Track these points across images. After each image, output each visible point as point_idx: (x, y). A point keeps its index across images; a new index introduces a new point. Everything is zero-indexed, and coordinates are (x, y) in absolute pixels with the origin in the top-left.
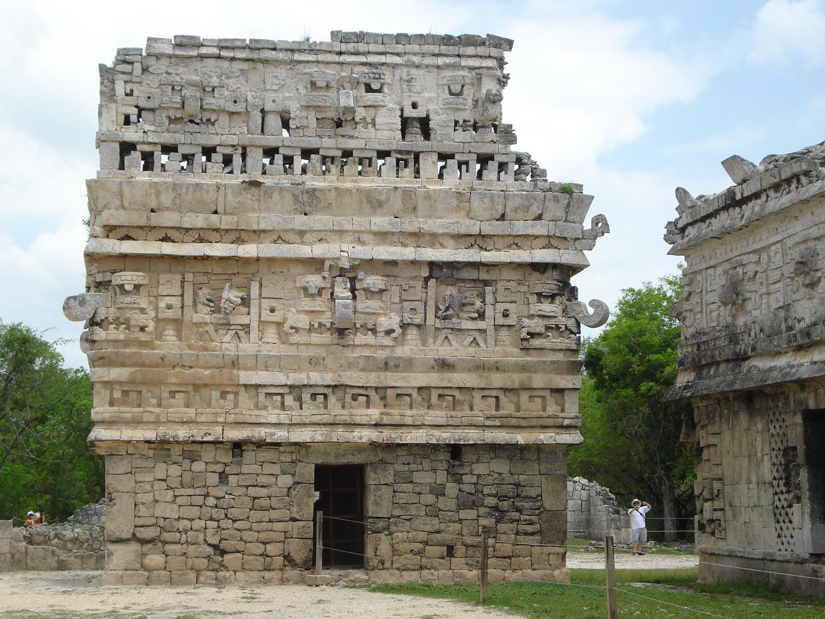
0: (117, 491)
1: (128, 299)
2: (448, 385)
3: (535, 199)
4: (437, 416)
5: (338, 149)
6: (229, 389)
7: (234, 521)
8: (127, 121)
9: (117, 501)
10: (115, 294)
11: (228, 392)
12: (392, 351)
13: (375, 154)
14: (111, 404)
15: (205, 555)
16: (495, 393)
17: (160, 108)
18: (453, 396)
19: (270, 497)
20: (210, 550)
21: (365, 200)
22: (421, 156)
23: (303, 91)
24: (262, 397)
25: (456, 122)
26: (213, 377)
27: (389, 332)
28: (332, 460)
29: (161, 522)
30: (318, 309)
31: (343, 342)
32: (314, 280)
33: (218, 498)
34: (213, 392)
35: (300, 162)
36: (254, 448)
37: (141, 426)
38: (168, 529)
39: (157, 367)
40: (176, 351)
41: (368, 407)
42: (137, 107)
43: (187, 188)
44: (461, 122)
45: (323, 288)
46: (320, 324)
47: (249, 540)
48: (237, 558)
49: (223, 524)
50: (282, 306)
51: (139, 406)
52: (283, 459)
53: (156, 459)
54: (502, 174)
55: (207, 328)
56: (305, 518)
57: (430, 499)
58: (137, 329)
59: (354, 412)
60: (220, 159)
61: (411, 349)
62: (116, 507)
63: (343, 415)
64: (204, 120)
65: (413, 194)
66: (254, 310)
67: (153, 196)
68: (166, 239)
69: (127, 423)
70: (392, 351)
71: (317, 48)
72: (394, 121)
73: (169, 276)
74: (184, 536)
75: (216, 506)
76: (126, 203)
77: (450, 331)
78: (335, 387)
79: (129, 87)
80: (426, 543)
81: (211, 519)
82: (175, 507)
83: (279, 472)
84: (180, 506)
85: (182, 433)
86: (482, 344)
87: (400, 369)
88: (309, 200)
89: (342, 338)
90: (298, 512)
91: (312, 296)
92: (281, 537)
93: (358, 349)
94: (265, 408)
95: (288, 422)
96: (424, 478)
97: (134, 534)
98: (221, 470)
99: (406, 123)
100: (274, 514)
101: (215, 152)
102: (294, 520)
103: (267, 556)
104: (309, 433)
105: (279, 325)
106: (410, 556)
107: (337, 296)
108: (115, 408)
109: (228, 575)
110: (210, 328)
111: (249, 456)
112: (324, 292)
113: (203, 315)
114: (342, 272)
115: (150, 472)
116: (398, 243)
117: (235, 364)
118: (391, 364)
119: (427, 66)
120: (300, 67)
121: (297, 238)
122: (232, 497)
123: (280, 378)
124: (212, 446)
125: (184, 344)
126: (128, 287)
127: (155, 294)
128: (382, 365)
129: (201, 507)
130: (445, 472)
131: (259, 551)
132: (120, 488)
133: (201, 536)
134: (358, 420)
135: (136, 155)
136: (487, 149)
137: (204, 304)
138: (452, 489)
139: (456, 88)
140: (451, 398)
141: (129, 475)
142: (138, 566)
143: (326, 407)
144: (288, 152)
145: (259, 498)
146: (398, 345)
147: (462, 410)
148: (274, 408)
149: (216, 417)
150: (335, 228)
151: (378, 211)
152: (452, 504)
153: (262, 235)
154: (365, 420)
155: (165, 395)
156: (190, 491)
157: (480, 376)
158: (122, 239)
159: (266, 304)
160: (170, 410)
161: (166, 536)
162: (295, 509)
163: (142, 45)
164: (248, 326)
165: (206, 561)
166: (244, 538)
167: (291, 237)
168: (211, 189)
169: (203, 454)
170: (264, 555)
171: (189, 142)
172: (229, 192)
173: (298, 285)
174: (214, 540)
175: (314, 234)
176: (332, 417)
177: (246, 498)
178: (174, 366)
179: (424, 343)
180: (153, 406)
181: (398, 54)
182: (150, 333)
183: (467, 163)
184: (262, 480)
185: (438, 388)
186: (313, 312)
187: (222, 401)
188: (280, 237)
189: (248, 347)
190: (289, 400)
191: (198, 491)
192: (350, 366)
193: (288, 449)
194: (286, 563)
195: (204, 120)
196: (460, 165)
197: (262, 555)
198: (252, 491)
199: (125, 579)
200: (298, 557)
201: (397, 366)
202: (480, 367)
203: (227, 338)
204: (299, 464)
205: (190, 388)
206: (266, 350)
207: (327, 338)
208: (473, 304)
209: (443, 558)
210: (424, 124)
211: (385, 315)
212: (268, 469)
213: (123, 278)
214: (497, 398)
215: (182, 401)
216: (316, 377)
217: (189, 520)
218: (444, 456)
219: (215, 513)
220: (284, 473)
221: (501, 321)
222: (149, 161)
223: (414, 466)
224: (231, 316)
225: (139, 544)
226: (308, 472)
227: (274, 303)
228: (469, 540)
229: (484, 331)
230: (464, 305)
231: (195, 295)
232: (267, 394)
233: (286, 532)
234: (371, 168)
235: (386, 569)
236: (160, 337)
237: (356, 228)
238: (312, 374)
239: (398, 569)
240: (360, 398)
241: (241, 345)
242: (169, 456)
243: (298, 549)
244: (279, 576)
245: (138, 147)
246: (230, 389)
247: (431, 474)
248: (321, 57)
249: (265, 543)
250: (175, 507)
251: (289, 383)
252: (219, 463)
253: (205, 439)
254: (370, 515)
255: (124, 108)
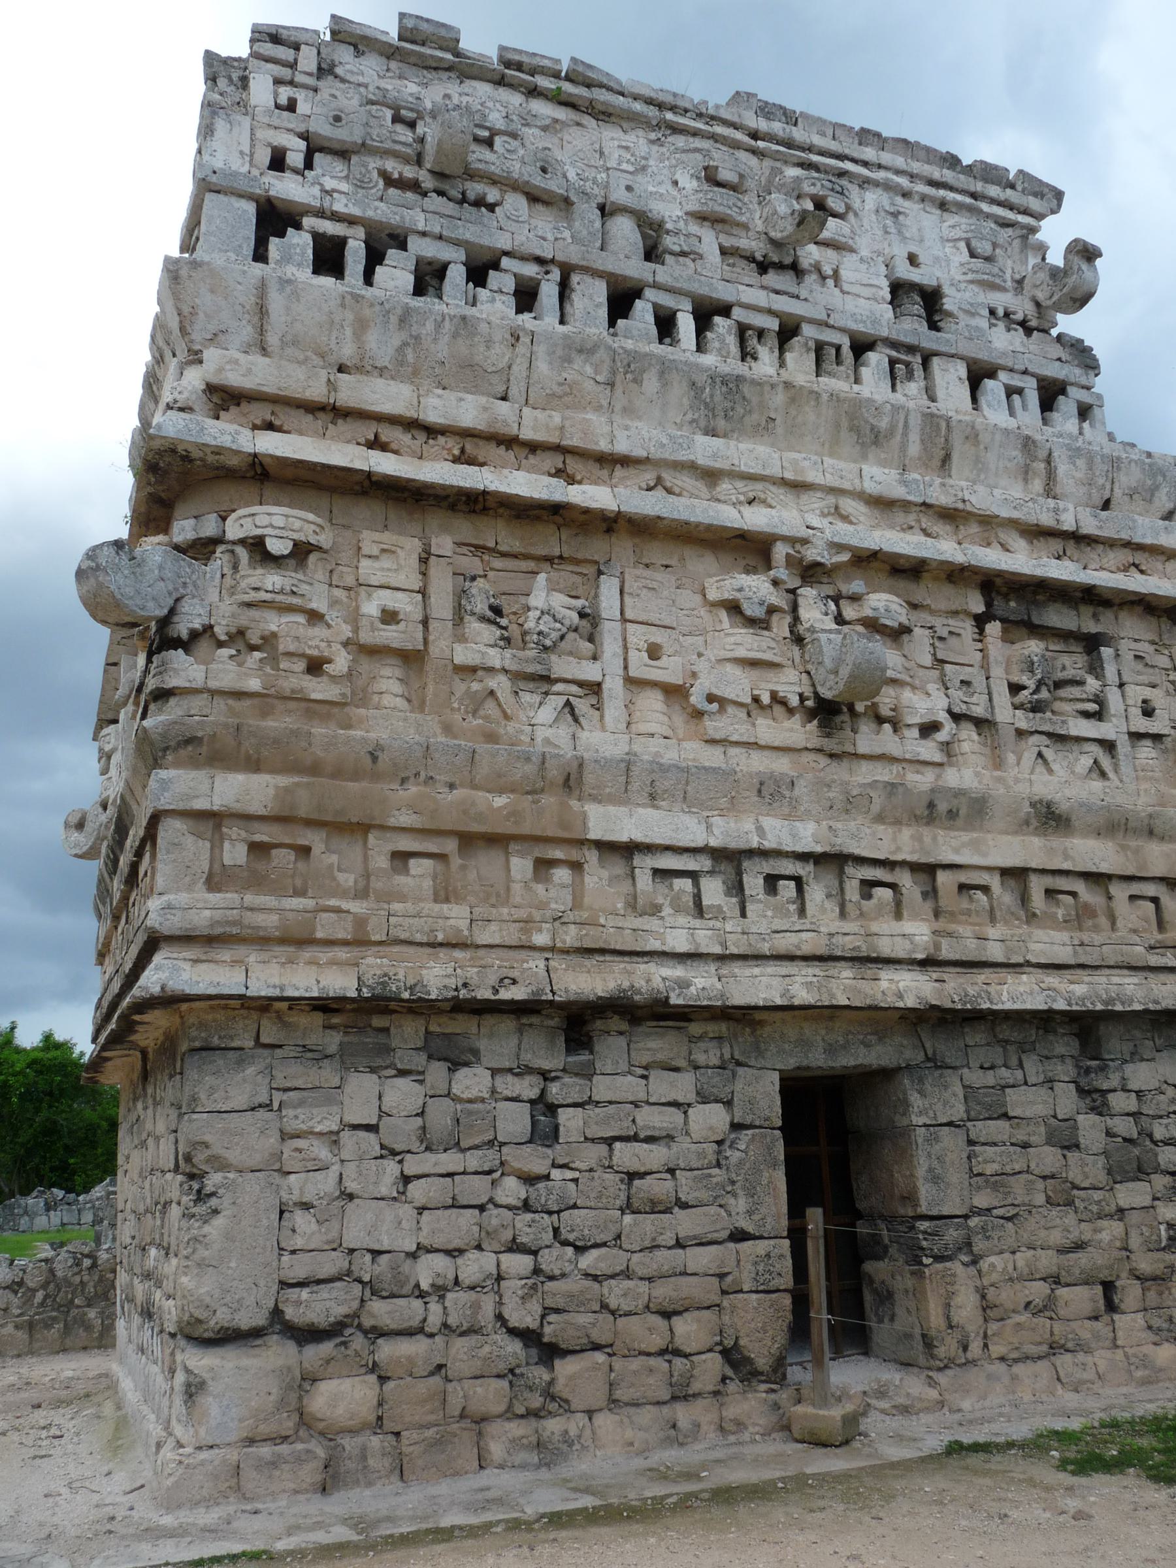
0: (222, 1165)
1: (273, 580)
2: (1066, 866)
3: (1164, 476)
4: (1050, 943)
5: (770, 312)
6: (558, 854)
7: (580, 1250)
8: (278, 162)
9: (223, 1202)
10: (235, 567)
11: (552, 863)
12: (939, 777)
13: (846, 342)
14: (213, 883)
15: (502, 1367)
16: (1150, 890)
17: (363, 148)
18: (1074, 894)
19: (671, 1171)
20: (515, 1347)
21: (845, 423)
22: (936, 362)
23: (688, 183)
24: (644, 880)
25: (992, 312)
26: (514, 814)
27: (928, 729)
28: (818, 1059)
29: (365, 1267)
30: (768, 656)
31: (831, 745)
32: (756, 588)
33: (530, 1180)
34: (515, 862)
35: (686, 324)
36: (624, 1026)
37: (307, 953)
38: (387, 1287)
39: (356, 776)
40: (412, 736)
41: (898, 916)
42: (305, 136)
43: (439, 325)
44: (1001, 312)
45: (772, 610)
46: (774, 695)
47: (625, 1308)
48: (596, 1367)
49: (551, 1259)
50: (677, 647)
51: (300, 893)
52: (701, 1058)
53: (346, 1060)
54: (1086, 425)
55: (492, 683)
56: (767, 1230)
57: (1048, 1158)
58: (301, 666)
59: (875, 927)
60: (510, 285)
61: (977, 774)
62: (219, 1221)
63: (849, 935)
64: (471, 196)
65: (943, 425)
66: (610, 646)
67: (348, 332)
68: (375, 444)
69: (262, 941)
70: (939, 777)
71: (711, 111)
72: (875, 282)
73: (388, 538)
74: (435, 1307)
75: (526, 1206)
76: (273, 340)
77: (1044, 740)
78: (818, 859)
79: (285, 93)
80: (1056, 1280)
81: (515, 1247)
82: (406, 1212)
83: (691, 1097)
84: (421, 1210)
85: (437, 977)
86: (1111, 775)
87: (959, 822)
88: (724, 405)
89: (828, 735)
90: (750, 1213)
91: (752, 622)
92: (706, 1290)
93: (865, 766)
94: (655, 910)
95: (717, 950)
96: (1028, 1102)
97: (277, 1312)
98: (533, 1093)
99: (899, 290)
100: (685, 1223)
101: (496, 266)
102: (739, 1236)
103: (678, 1353)
104: (775, 982)
105: (675, 693)
106: (1023, 1318)
107: (812, 630)
108: (229, 897)
109: (575, 1424)
110: (501, 684)
111: (611, 1049)
112: (775, 618)
113: (480, 645)
114: (811, 572)
115: (329, 1101)
116: (917, 530)
117: (571, 781)
118: (942, 807)
119: (923, 198)
120: (680, 141)
121: (701, 486)
122: (570, 1175)
123: (690, 829)
124: (508, 1024)
125: (432, 724)
126: (276, 546)
127: (350, 581)
128: (922, 811)
129: (482, 1208)
130: (1072, 1086)
131: (657, 1342)
132: (233, 1156)
133: (488, 1305)
134: (886, 948)
135: (300, 242)
136: (1055, 371)
137: (483, 619)
138: (1090, 1128)
139: (984, 247)
140: (1069, 899)
141: (262, 1114)
142: (288, 1424)
143: (802, 912)
144: (667, 300)
145: (642, 1175)
146: (951, 765)
147: (1096, 929)
148: (678, 910)
149: (527, 932)
150: (789, 475)
151: (872, 452)
152: (1096, 1171)
153: (619, 472)
154: (900, 949)
155: (381, 862)
156: (450, 1161)
157: (1124, 848)
158: (255, 427)
159: (638, 636)
160: (396, 907)
161: (381, 1312)
162: (740, 1204)
163: (321, 25)
164: (594, 689)
165: (504, 1384)
166: (613, 1304)
167: (685, 481)
168: (497, 337)
169: (483, 1045)
170: (670, 1351)
171: (437, 230)
172: (541, 349)
173: (713, 595)
174: (524, 1316)
175: (740, 484)
176: (824, 940)
177: (611, 1178)
178: (404, 781)
179: (998, 763)
180: (344, 894)
181: (865, 164)
182: (334, 678)
183: (1020, 391)
184: (652, 1119)
185: (1043, 871)
186: (754, 663)
187: (540, 888)
188: (659, 481)
189: (601, 740)
190: (713, 891)
191: (473, 1161)
192: (850, 804)
193: (712, 1028)
194: (730, 1372)
195: (471, 196)
196: (1011, 391)
197: (662, 1352)
198: (626, 1155)
199: (250, 1477)
200: (762, 1347)
201: (952, 814)
202: (1115, 826)
203: (546, 714)
204: (741, 1071)
205: (450, 846)
206: (647, 749)
207: (799, 731)
208: (1081, 683)
209: (1096, 1318)
210: (931, 299)
211: (914, 688)
212: (664, 1086)
213: (262, 520)
214: (1155, 900)
215: (428, 884)
216: (778, 831)
217: (448, 1253)
218: (1066, 1045)
219: (526, 1227)
220: (704, 1098)
221: (1141, 724)
222: (328, 258)
223: (1004, 1072)
224: (554, 658)
225: (291, 1347)
226: (762, 1093)
227: (658, 636)
228: (1146, 1264)
229: (1109, 746)
230: (1058, 685)
231: (461, 594)
232: (657, 872)
233: (722, 1276)
234: (842, 368)
235: (973, 1362)
236: (362, 698)
237: (830, 480)
238: (768, 822)
239: (1002, 1359)
240: (879, 892)
241: (584, 735)
242: (388, 1050)
243: (760, 1325)
244: (713, 1416)
245: (307, 222)
246: (562, 851)
247: (1043, 1091)
248: (719, 129)
249: (667, 1315)
250: (406, 1212)
251: (713, 843)
252: (529, 1070)
253: (505, 995)
254: (923, 1209)
255: (272, 132)
